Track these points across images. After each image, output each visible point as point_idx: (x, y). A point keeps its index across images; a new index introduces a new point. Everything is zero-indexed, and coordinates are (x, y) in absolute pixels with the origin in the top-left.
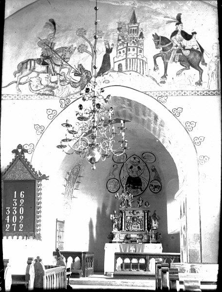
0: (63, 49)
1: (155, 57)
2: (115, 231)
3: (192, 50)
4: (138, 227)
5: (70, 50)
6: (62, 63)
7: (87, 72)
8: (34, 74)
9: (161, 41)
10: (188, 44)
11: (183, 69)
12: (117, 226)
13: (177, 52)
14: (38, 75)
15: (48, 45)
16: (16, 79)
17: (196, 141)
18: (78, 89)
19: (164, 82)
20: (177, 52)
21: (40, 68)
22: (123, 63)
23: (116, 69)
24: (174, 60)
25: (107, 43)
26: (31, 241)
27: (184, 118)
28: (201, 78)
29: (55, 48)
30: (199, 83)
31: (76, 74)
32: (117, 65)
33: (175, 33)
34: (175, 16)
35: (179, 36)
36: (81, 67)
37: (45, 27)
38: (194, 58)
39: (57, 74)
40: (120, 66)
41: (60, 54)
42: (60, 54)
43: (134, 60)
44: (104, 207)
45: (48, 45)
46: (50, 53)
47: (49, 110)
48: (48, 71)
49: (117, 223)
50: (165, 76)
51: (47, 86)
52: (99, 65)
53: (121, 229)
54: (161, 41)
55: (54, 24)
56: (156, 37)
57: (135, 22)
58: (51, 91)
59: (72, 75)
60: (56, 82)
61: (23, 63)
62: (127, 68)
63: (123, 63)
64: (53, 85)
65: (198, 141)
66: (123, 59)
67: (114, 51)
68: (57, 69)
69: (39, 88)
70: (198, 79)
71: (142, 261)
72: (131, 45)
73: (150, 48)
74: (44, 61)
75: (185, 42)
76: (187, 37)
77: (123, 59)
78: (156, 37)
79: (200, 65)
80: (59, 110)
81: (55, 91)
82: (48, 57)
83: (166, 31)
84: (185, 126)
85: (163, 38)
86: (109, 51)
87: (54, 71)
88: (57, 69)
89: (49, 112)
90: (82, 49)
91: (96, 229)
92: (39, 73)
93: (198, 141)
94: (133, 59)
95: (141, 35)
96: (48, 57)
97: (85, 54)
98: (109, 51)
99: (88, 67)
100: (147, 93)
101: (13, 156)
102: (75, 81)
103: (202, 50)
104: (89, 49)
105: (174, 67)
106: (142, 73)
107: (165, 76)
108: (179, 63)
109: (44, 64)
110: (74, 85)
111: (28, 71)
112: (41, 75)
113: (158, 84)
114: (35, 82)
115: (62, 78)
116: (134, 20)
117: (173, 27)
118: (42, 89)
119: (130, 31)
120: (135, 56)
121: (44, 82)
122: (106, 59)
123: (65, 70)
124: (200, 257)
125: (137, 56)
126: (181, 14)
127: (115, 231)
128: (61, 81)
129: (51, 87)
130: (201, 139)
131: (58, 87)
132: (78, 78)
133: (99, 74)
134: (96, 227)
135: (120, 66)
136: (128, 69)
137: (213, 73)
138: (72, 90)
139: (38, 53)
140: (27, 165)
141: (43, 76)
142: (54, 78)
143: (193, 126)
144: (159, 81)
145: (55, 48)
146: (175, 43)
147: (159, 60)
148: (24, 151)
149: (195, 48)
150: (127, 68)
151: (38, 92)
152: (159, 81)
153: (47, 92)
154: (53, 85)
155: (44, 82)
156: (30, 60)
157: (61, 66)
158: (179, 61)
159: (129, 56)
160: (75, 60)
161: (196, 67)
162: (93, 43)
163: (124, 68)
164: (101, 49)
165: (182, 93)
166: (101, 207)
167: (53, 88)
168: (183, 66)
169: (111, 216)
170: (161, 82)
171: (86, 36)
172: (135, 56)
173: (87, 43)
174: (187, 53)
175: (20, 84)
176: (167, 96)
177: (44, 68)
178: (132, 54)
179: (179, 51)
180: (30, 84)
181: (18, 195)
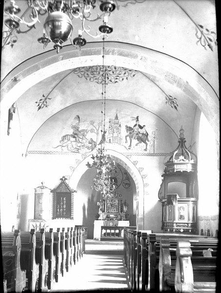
0: (83, 130)
1: (126, 137)
2: (100, 212)
3: (143, 134)
8: (69, 142)
9: (129, 129)
10: (142, 131)
12: (101, 210)
13: (137, 135)
15: (76, 128)
16: (61, 144)
19: (129, 149)
20: (137, 135)
21: (73, 139)
23: (108, 141)
26: (51, 216)
27: (138, 166)
28: (147, 146)
30: (146, 150)
31: (90, 143)
32: (109, 139)
33: (135, 125)
34: (136, 117)
35: (137, 127)
37: (75, 119)
40: (110, 140)
41: (82, 133)
42: (82, 133)
44: (93, 197)
45: (76, 128)
46: (77, 132)
49: (101, 208)
50: (130, 146)
52: (100, 138)
53: (104, 211)
54: (129, 129)
56: (127, 127)
57: (117, 119)
59: (88, 143)
60: (80, 147)
61: (64, 137)
63: (111, 139)
64: (79, 148)
67: (107, 132)
68: (80, 140)
70: (145, 148)
71: (117, 231)
72: (115, 130)
73: (124, 133)
75: (140, 130)
76: (141, 127)
78: (127, 127)
80: (81, 160)
82: (76, 134)
83: (132, 124)
85: (130, 127)
88: (80, 140)
90: (92, 131)
91: (88, 211)
95: (120, 125)
96: (76, 134)
99: (95, 140)
101: (60, 181)
103: (148, 134)
104: (96, 131)
105: (135, 141)
107: (130, 146)
109: (74, 137)
110: (88, 148)
111: (66, 141)
114: (70, 146)
115: (83, 145)
116: (117, 118)
117: (134, 122)
119: (115, 124)
122: (103, 136)
123: (84, 141)
127: (100, 212)
132: (90, 145)
134: (88, 209)
135: (110, 140)
138: (88, 151)
139: (71, 132)
140: (67, 186)
141: (74, 143)
142: (79, 145)
146: (136, 130)
147: (128, 138)
148: (66, 179)
149: (144, 133)
154: (79, 148)
155: (75, 147)
156: (68, 135)
159: (114, 136)
160: (89, 136)
161: (145, 142)
162: (97, 128)
163: (112, 141)
166: (91, 196)
171: (94, 125)
173: (95, 129)
174: (140, 135)
175: (63, 146)
177: (74, 139)
178: (115, 135)
179: (137, 134)
181: (63, 199)
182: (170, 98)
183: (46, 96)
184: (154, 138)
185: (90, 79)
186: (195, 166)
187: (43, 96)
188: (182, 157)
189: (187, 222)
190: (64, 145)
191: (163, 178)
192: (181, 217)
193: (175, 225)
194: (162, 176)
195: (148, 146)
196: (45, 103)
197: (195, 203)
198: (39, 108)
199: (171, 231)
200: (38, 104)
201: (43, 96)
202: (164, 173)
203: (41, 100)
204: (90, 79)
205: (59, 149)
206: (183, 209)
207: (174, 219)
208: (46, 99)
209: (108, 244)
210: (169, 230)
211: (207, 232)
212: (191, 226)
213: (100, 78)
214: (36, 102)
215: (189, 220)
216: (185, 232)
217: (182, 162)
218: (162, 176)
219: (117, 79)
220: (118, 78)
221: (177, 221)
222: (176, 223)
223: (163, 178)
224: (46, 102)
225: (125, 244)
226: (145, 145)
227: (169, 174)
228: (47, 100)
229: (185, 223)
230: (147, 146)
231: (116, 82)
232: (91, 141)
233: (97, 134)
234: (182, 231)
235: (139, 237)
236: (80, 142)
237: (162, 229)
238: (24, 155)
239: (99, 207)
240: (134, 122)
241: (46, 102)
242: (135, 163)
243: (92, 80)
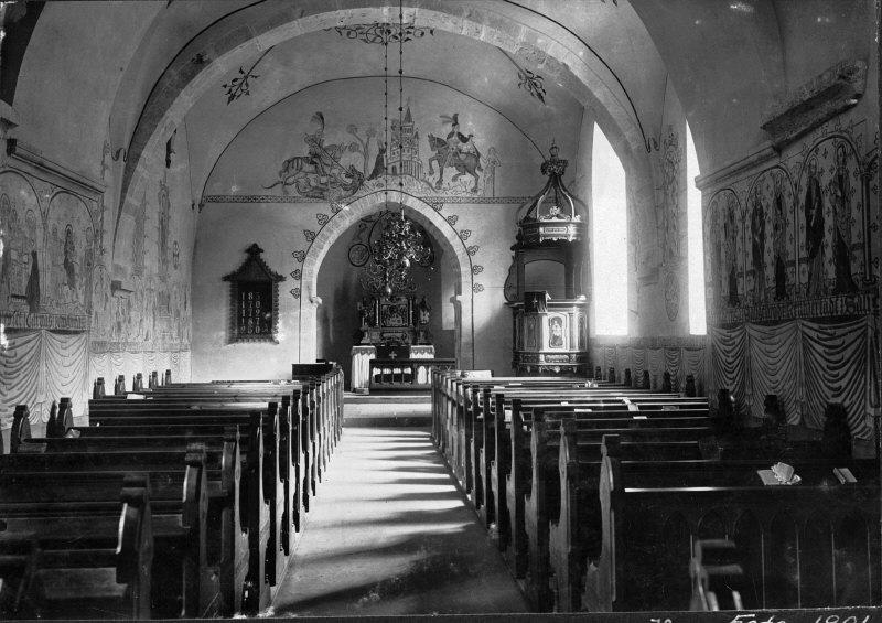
1: (431, 160)
5: (340, 149)
7: (360, 174)
8: (302, 174)
9: (437, 143)
10: (465, 147)
12: (367, 320)
15: (315, 141)
18: (350, 192)
21: (308, 168)
23: (390, 171)
25: (380, 143)
27: (459, 226)
28: (477, 180)
29: (326, 144)
30: (475, 190)
31: (348, 176)
32: (390, 167)
34: (451, 115)
35: (455, 138)
36: (353, 169)
38: (471, 162)
40: (394, 168)
45: (315, 141)
46: (318, 151)
48: (316, 171)
50: (440, 182)
51: (317, 187)
54: (437, 143)
55: (322, 118)
56: (432, 138)
60: (326, 184)
70: (473, 186)
73: (425, 152)
74: (314, 159)
75: (461, 144)
76: (464, 139)
78: (432, 138)
81: (325, 193)
83: (444, 131)
85: (439, 140)
86: (383, 151)
88: (327, 169)
90: (353, 147)
96: (316, 156)
97: (356, 154)
98: (383, 151)
99: (360, 169)
103: (479, 155)
105: (451, 172)
109: (312, 163)
117: (449, 128)
121: (313, 184)
122: (379, 161)
123: (336, 171)
126: (456, 115)
127: (365, 326)
128: (331, 183)
132: (349, 181)
133: (372, 177)
135: (394, 168)
138: (343, 193)
139: (305, 151)
141: (311, 177)
142: (324, 180)
145: (326, 144)
146: (452, 145)
147: (435, 163)
149: (471, 151)
152: (434, 185)
155: (313, 184)
156: (297, 158)
157: (332, 167)
159: (404, 158)
160: (346, 160)
161: (472, 172)
162: (365, 141)
163: (398, 172)
164: (374, 150)
165: (456, 201)
169: (359, 304)
173: (358, 143)
174: (462, 157)
177: (312, 168)
179: (456, 155)
180: (297, 186)
182: (528, 74)
183: (246, 71)
184: (494, 163)
185: (349, 34)
186: (583, 228)
187: (241, 71)
188: (555, 210)
189: (567, 351)
190: (291, 180)
191: (513, 253)
192: (555, 341)
193: (542, 357)
194: (512, 249)
195: (481, 181)
196: (244, 87)
197: (584, 308)
198: (231, 99)
199: (535, 372)
200: (228, 89)
201: (241, 71)
202: (516, 242)
203: (235, 80)
204: (349, 34)
205: (278, 191)
206: (559, 321)
207: (540, 346)
208: (246, 77)
209: (401, 402)
210: (529, 369)
211: (608, 371)
212: (578, 360)
213: (372, 31)
214: (225, 86)
215: (572, 347)
216: (564, 372)
217: (555, 220)
218: (512, 249)
219: (408, 32)
220: (412, 31)
221: (546, 349)
222: (546, 354)
223: (513, 253)
224: (247, 85)
225: (436, 402)
226: (473, 178)
227: (527, 241)
228: (250, 80)
229: (563, 354)
230: (477, 180)
231: (408, 39)
232: (352, 172)
233: (366, 155)
234: (557, 370)
235: (465, 388)
236: (325, 175)
237: (515, 365)
238: (197, 207)
239: (362, 313)
240: (449, 128)
241: (247, 85)
242: (451, 221)
243: (353, 34)
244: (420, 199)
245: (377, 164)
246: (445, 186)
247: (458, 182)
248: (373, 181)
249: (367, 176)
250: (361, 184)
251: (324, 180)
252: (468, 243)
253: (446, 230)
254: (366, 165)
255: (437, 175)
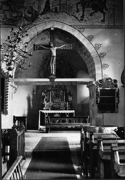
2: (45, 102)
4: (59, 100)
6: (20, 5)
7: (35, 11)
11: (94, 13)
12: (46, 100)
14: (4, 12)
17: (101, 56)
18: (30, 22)
19: (82, 20)
22: (58, 7)
23: (54, 10)
24: (88, 6)
30: (103, 21)
31: (29, 13)
39: (17, 12)
40: (56, 8)
43: (64, 5)
47: (11, 35)
49: (46, 98)
50: (83, 16)
51: (10, 19)
52: (43, 6)
53: (49, 101)
58: (13, 23)
59: (26, 13)
60: (16, 17)
62: (60, 10)
63: (58, 7)
65: (102, 55)
66: (57, 5)
69: (5, 20)
70: (102, 18)
77: (57, 5)
79: (104, 10)
84: (94, 46)
87: (14, 10)
89: (12, 36)
91: (32, 102)
92: (5, 11)
93: (102, 55)
94: (64, 4)
100: (73, 26)
102: (28, 17)
106: (69, 14)
108: (91, 9)
109: (8, 5)
110: (27, 18)
112: (6, 12)
113: (79, 21)
118: (7, 21)
120: (65, 3)
121: (8, 17)
124: (102, 122)
125: (67, 3)
127: (45, 102)
128: (19, 16)
129: (13, 20)
130: (104, 54)
131: (17, 20)
132: (30, 16)
133: (43, 14)
134: (32, 100)
136: (61, 11)
137: (111, 15)
138: (26, 22)
142: (15, 15)
143: (100, 46)
144: (79, 19)
147: (80, 7)
150: (60, 10)
151: (4, 23)
152: (79, 19)
153: (11, 23)
158: (91, 7)
161: (102, 11)
167: (14, 21)
168: (94, 10)
169: (43, 93)
170: (81, 20)
172: (65, 3)
176: (84, 28)
184: (114, 5)
226: (102, 15)
239: (44, 97)
242: (90, 39)
244: (71, 26)
245: (46, 6)
246: (85, 18)
247: (93, 17)
248: (44, 16)
249: (40, 12)
250: (37, 17)
251: (15, 15)
252: (100, 51)
253: (85, 43)
254: (39, 8)
255: (81, 13)
